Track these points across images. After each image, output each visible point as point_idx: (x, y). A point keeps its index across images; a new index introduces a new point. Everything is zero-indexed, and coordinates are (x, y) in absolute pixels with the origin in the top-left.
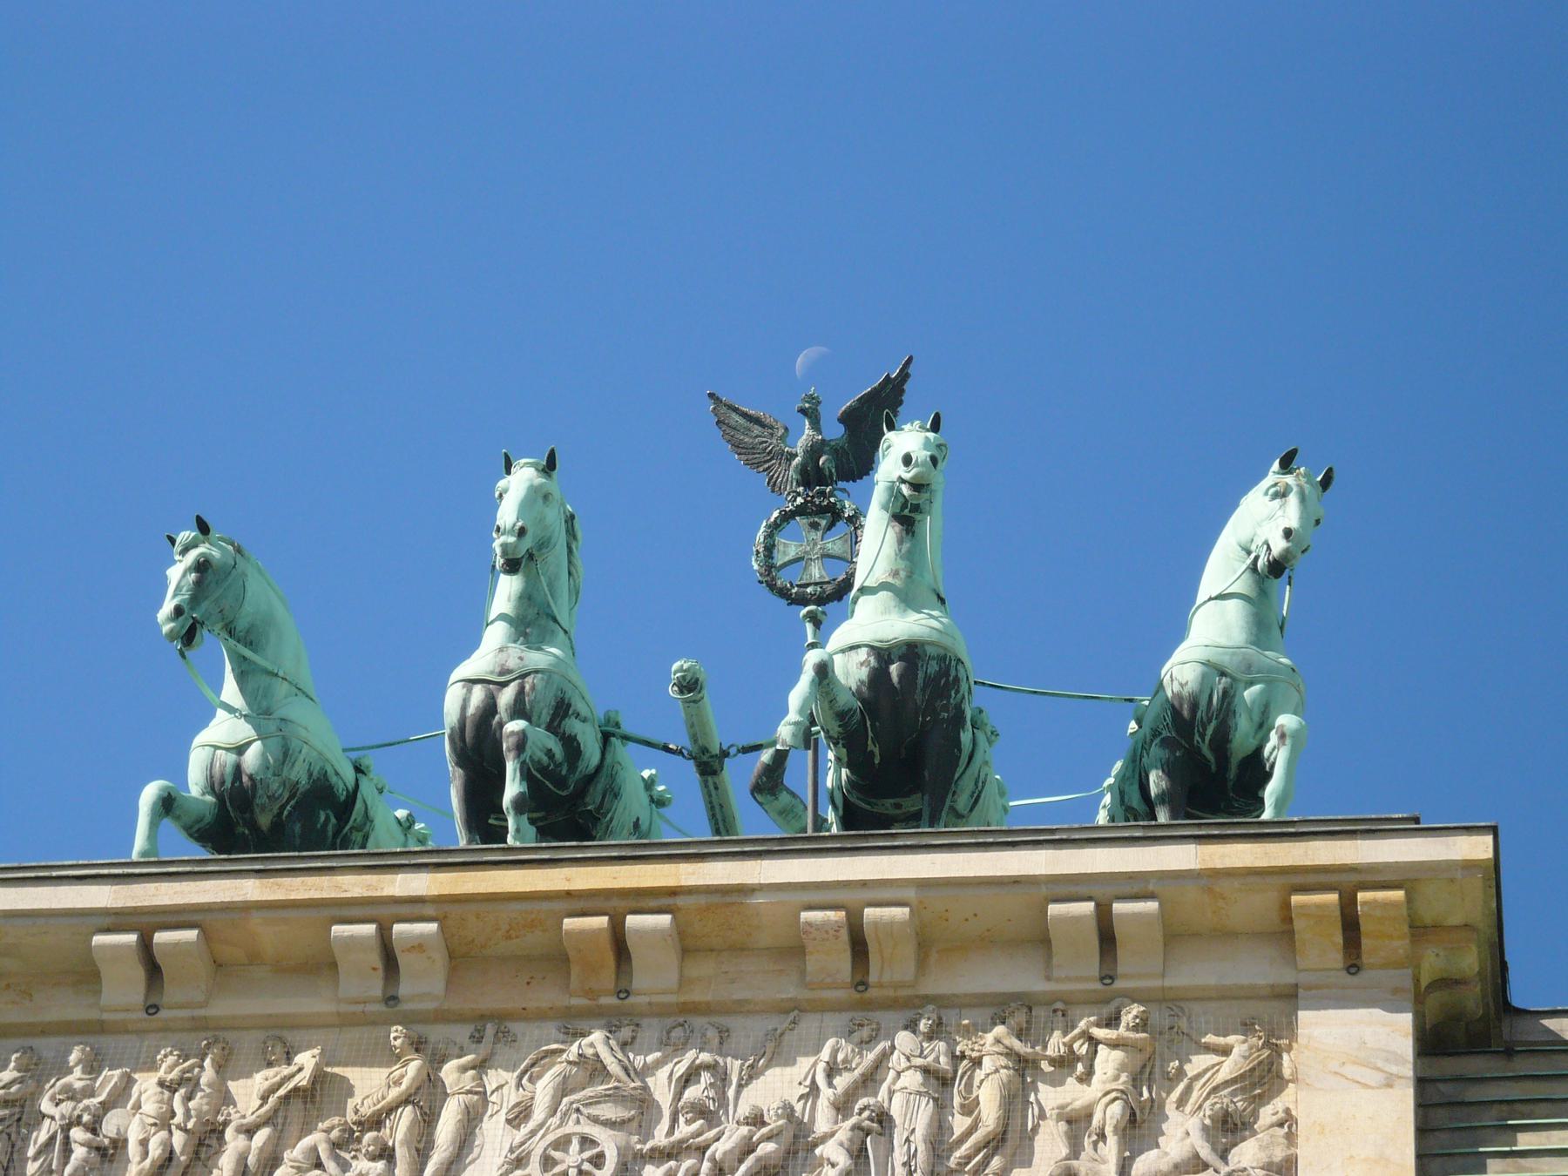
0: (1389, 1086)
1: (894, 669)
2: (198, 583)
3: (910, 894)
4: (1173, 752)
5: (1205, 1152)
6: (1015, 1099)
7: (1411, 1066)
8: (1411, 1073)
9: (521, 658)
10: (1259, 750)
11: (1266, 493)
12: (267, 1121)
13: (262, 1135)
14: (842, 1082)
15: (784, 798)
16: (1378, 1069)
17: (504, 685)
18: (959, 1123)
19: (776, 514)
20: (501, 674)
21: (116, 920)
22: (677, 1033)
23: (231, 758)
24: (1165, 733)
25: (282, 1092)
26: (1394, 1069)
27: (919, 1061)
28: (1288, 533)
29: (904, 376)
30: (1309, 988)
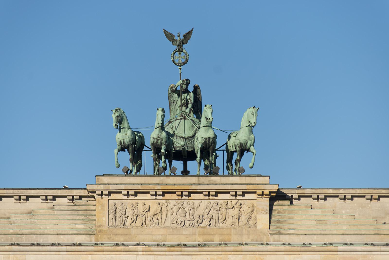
0: (266, 214)
1: (207, 140)
2: (117, 119)
3: (215, 190)
4: (240, 148)
5: (247, 223)
6: (226, 214)
7: (269, 211)
8: (268, 212)
9: (161, 136)
10: (250, 148)
11: (252, 113)
12: (145, 215)
13: (144, 217)
14: (208, 211)
15: (176, 92)
16: (265, 212)
17: (159, 139)
18: (220, 217)
19: (174, 52)
20: (158, 138)
21: (125, 190)
22: (189, 203)
23: (122, 141)
24: (239, 146)
25: (145, 211)
26: (267, 212)
27: (216, 210)
28: (254, 122)
29: (192, 30)
30: (258, 200)
